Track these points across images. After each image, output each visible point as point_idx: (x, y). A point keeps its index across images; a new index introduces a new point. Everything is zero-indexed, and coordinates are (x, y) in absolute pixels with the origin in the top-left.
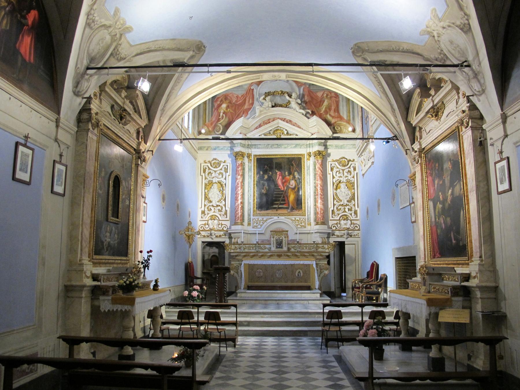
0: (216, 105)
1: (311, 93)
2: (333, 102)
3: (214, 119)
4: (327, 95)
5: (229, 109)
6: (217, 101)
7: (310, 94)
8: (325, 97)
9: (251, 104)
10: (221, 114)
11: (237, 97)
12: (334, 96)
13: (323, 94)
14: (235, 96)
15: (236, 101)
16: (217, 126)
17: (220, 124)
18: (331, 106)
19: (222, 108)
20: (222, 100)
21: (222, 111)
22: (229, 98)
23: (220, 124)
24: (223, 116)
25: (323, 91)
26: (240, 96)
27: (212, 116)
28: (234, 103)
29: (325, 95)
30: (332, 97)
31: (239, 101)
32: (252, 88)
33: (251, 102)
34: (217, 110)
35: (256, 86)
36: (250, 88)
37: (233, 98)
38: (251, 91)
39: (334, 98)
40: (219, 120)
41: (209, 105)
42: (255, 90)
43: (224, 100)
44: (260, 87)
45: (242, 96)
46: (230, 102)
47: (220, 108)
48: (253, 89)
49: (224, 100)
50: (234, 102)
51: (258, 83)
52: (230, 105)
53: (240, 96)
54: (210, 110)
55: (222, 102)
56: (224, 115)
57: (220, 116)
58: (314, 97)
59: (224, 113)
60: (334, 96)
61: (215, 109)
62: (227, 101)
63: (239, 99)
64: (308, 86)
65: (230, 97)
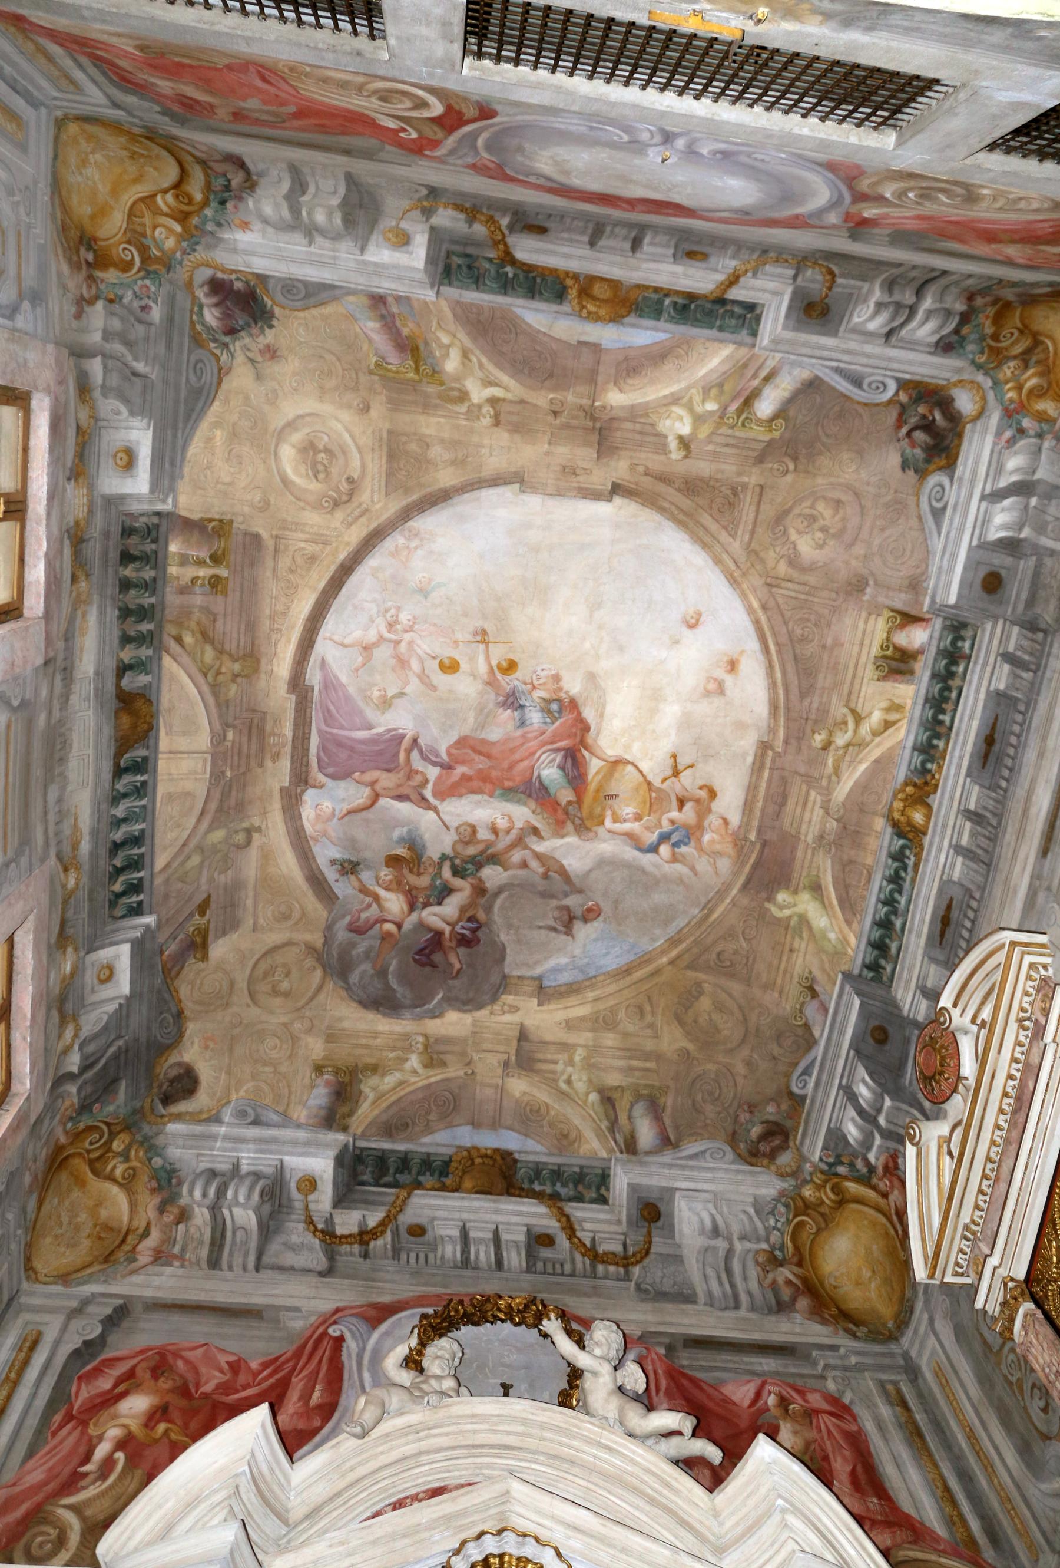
0: (84, 1394)
1: (685, 1382)
2: (829, 1432)
3: (36, 1476)
4: (784, 1402)
5: (162, 1427)
6: (97, 1371)
7: (680, 1388)
8: (775, 1412)
9: (319, 1407)
10: (102, 1451)
11: (236, 1367)
12: (826, 1407)
13: (758, 1395)
14: (223, 1359)
15: (226, 1388)
16: (45, 1521)
17: (71, 1507)
18: (826, 1458)
19: (115, 1416)
20: (131, 1374)
21: (114, 1433)
22: (180, 1363)
23: (65, 1507)
24: (108, 1463)
25: (759, 1382)
26: (254, 1365)
27: (30, 1454)
28: (206, 1396)
29: (772, 1400)
30: (817, 1412)
31: (245, 1387)
32: (334, 1331)
33: (316, 1397)
34: (85, 1424)
35: (363, 1327)
36: (325, 1333)
37: (203, 1370)
38: (327, 1346)
39: (827, 1421)
40: (73, 1482)
41: (34, 1396)
42: (351, 1345)
43: (143, 1374)
44: (387, 1334)
45: (265, 1365)
46: (184, 1391)
47: (112, 1410)
48: (341, 1339)
49: (143, 1374)
50: (208, 1388)
51: (372, 1313)
52: (177, 1401)
53: (254, 1365)
54: (33, 1421)
55: (128, 1383)
56: (120, 1456)
57: (87, 1459)
58: (711, 1405)
59: (121, 1445)
60: (826, 1407)
61: (69, 1417)
62: (165, 1384)
63: (242, 1379)
64: (662, 1351)
65: (187, 1362)
